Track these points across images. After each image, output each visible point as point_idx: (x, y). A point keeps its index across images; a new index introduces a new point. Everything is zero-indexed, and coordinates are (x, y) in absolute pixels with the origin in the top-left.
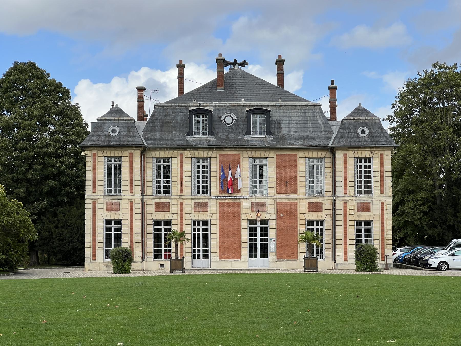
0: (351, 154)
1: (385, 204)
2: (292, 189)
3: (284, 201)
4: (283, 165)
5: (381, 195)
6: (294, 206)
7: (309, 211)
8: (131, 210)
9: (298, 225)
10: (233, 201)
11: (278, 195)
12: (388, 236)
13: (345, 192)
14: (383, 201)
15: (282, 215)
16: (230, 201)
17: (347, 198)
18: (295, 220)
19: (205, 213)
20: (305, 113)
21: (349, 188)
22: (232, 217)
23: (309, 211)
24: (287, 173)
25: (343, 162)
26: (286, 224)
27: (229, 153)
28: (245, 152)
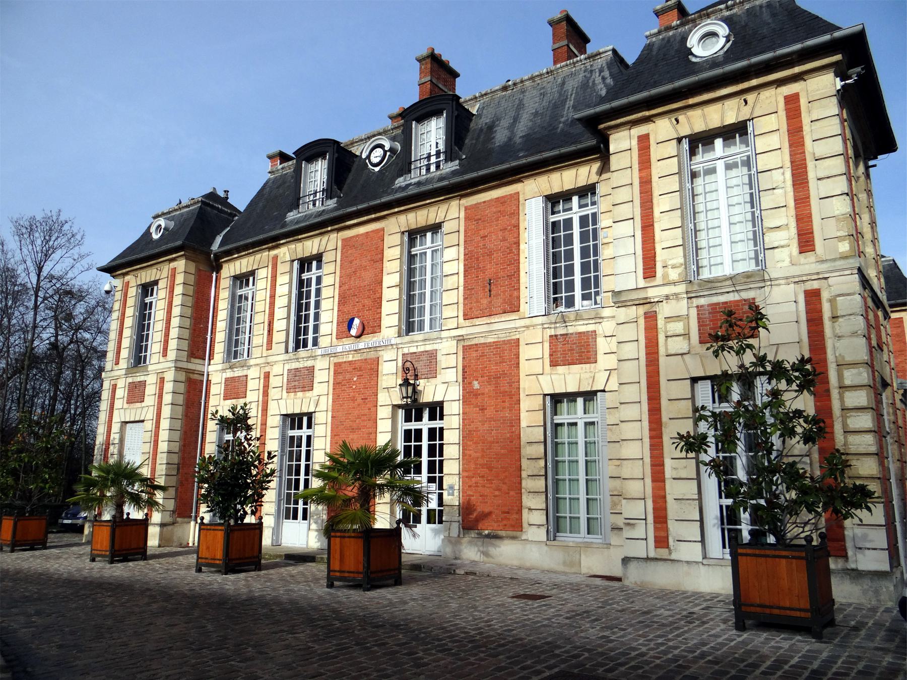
0: (662, 129)
1: (825, 295)
2: (505, 302)
3: (482, 341)
4: (482, 233)
5: (802, 258)
6: (508, 352)
7: (554, 364)
8: (160, 397)
9: (523, 415)
10: (364, 356)
11: (468, 323)
12: (852, 438)
13: (649, 271)
14: (815, 285)
15: (476, 385)
16: (358, 357)
17: (652, 293)
18: (512, 396)
19: (308, 394)
20: (563, 83)
21: (661, 256)
22: (359, 400)
23: (554, 364)
24: (490, 254)
25: (636, 166)
26: (489, 412)
27: (362, 230)
28: (392, 220)
